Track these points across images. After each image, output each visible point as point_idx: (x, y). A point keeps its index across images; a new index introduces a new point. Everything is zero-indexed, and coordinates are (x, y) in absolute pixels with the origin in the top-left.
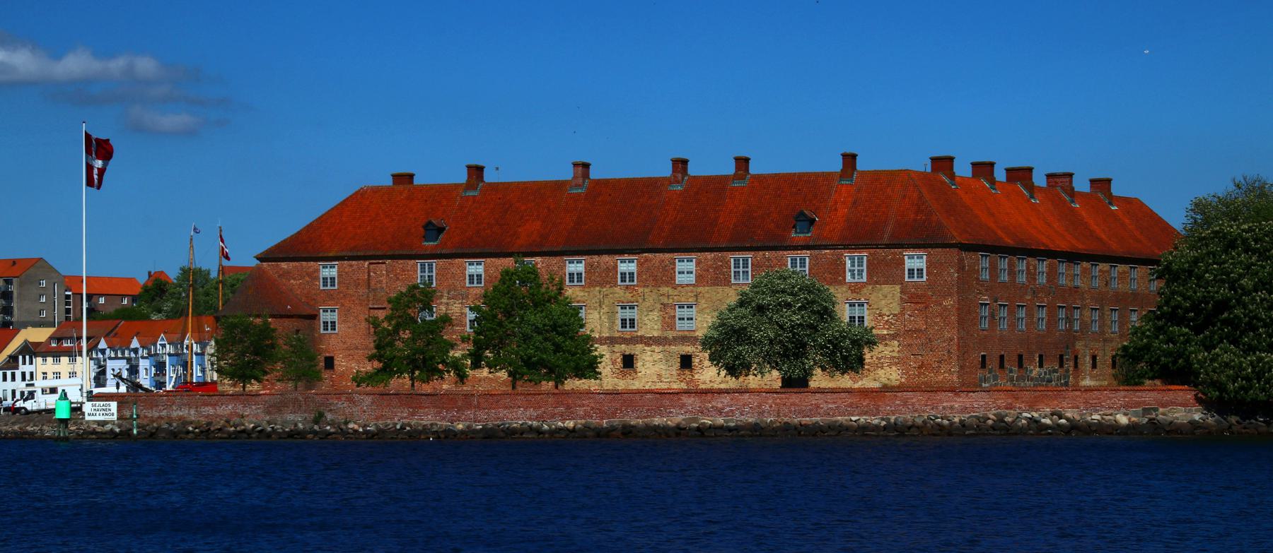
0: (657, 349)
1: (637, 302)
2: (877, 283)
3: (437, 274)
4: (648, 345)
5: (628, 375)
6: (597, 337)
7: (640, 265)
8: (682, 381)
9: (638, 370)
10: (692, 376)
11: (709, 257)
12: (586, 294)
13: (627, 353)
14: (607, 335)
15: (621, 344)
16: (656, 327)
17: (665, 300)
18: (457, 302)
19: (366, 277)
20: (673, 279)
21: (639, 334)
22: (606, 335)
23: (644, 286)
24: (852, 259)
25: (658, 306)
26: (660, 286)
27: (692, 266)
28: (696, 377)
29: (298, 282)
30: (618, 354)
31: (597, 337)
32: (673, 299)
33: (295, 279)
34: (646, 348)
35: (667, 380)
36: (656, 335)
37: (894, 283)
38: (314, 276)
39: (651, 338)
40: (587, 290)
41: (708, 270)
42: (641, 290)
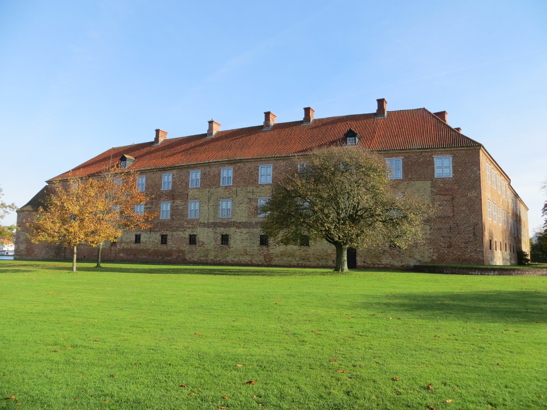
0: (245, 231)
1: (232, 197)
2: (411, 179)
4: (238, 228)
5: (224, 249)
6: (206, 222)
7: (235, 171)
9: (231, 246)
10: (268, 251)
11: (282, 164)
12: (201, 194)
13: (224, 234)
14: (212, 221)
15: (221, 227)
16: (244, 215)
17: (251, 196)
20: (256, 180)
21: (233, 220)
22: (211, 221)
23: (237, 186)
26: (248, 186)
27: (270, 170)
28: (271, 251)
30: (219, 235)
31: (206, 222)
32: (256, 195)
34: (237, 230)
35: (250, 254)
36: (244, 221)
37: (425, 179)
39: (240, 223)
40: (201, 190)
42: (234, 189)
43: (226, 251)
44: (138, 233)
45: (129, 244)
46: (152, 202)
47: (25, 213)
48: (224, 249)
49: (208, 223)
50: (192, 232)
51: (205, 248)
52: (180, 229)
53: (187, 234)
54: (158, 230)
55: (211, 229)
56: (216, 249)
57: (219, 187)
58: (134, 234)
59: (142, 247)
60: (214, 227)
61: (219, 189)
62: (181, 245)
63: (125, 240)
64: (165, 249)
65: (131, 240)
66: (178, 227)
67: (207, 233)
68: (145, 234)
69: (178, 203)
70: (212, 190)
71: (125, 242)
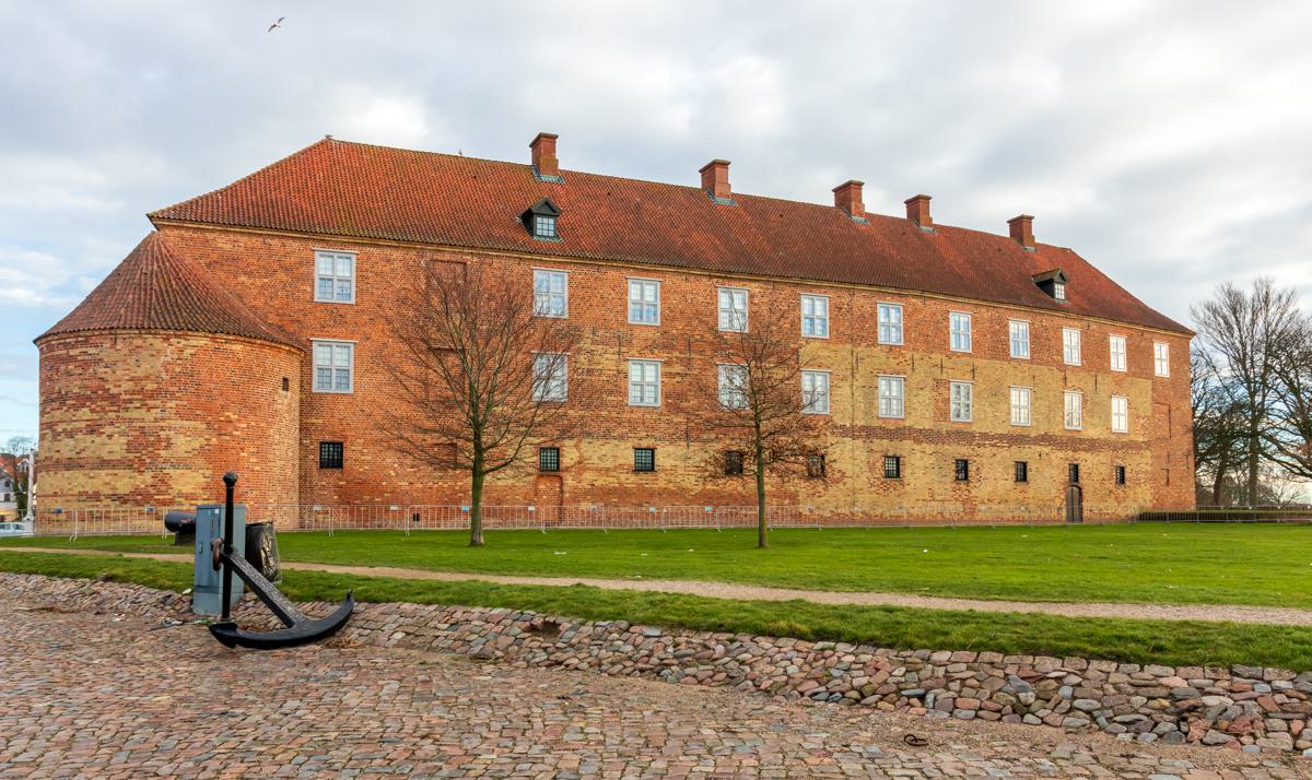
0: (929, 448)
1: (905, 373)
4: (919, 442)
5: (891, 489)
6: (848, 425)
8: (957, 500)
9: (906, 482)
11: (986, 315)
12: (833, 355)
14: (862, 423)
16: (927, 414)
18: (612, 351)
20: (947, 342)
22: (860, 423)
25: (930, 382)
26: (932, 352)
29: (258, 282)
30: (878, 455)
31: (848, 425)
33: (250, 274)
34: (915, 447)
35: (940, 498)
36: (927, 427)
38: (301, 273)
39: (921, 430)
40: (832, 347)
43: (897, 493)
47: (194, 343)
48: (891, 489)
49: (852, 427)
51: (848, 486)
55: (859, 442)
56: (873, 489)
57: (874, 343)
58: (629, 444)
60: (868, 436)
61: (876, 350)
63: (596, 461)
64: (740, 489)
65: (621, 461)
67: (853, 451)
68: (671, 449)
71: (598, 470)
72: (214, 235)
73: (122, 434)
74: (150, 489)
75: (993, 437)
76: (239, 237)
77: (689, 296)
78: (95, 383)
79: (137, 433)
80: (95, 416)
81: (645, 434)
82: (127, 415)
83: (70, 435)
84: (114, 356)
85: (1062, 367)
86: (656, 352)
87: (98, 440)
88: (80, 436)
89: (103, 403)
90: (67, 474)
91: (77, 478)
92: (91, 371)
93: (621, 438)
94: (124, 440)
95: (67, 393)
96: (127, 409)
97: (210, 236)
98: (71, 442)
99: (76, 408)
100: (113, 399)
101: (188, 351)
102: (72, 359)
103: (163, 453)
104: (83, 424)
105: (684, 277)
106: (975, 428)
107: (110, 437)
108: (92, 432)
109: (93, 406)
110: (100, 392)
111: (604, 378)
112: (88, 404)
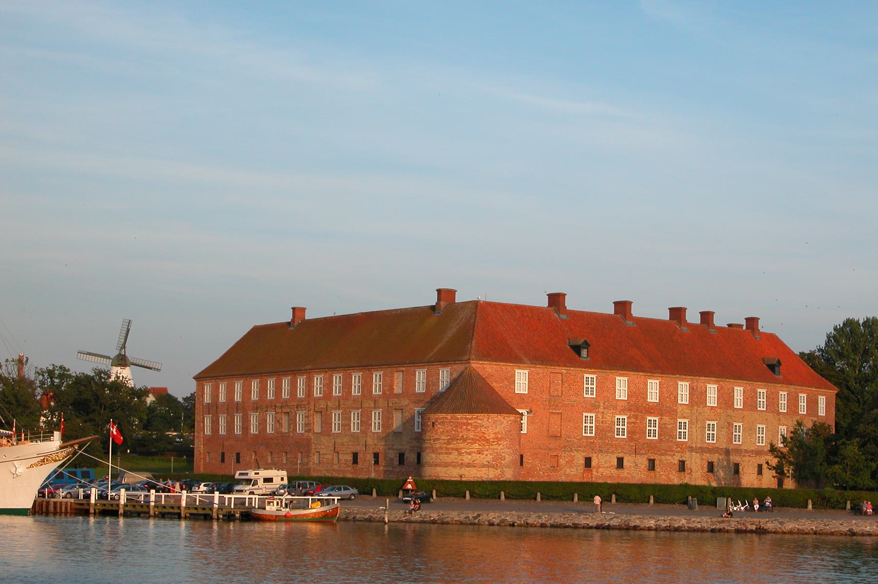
3: (597, 386)
13: (710, 461)
15: (707, 453)
19: (549, 385)
24: (821, 398)
26: (727, 409)
30: (705, 461)
31: (694, 447)
41: (748, 399)
42: (719, 411)
44: (620, 455)
45: (609, 469)
46: (637, 415)
49: (696, 447)
50: (681, 457)
52: (669, 453)
53: (675, 460)
54: (644, 452)
56: (702, 478)
58: (615, 456)
59: (626, 474)
61: (706, 409)
62: (670, 473)
63: (604, 463)
65: (612, 464)
66: (666, 450)
67: (695, 459)
68: (629, 458)
69: (666, 420)
70: (700, 409)
72: (486, 366)
73: (491, 454)
74: (499, 476)
75: (749, 452)
76: (493, 366)
77: (638, 385)
78: (481, 434)
79: (496, 454)
80: (481, 447)
81: (620, 451)
82: (491, 447)
83: (470, 454)
84: (489, 424)
85: (779, 414)
86: (625, 412)
87: (482, 457)
88: (474, 454)
89: (484, 442)
90: (467, 469)
91: (472, 471)
92: (479, 429)
93: (612, 452)
94: (491, 457)
95: (467, 438)
96: (492, 445)
97: (485, 366)
98: (470, 457)
99: (472, 444)
100: (487, 441)
101: (510, 422)
102: (471, 424)
103: (503, 462)
104: (476, 450)
105: (636, 376)
106: (743, 448)
107: (486, 455)
108: (479, 453)
109: (480, 443)
110: (483, 438)
111: (607, 425)
112: (478, 442)
